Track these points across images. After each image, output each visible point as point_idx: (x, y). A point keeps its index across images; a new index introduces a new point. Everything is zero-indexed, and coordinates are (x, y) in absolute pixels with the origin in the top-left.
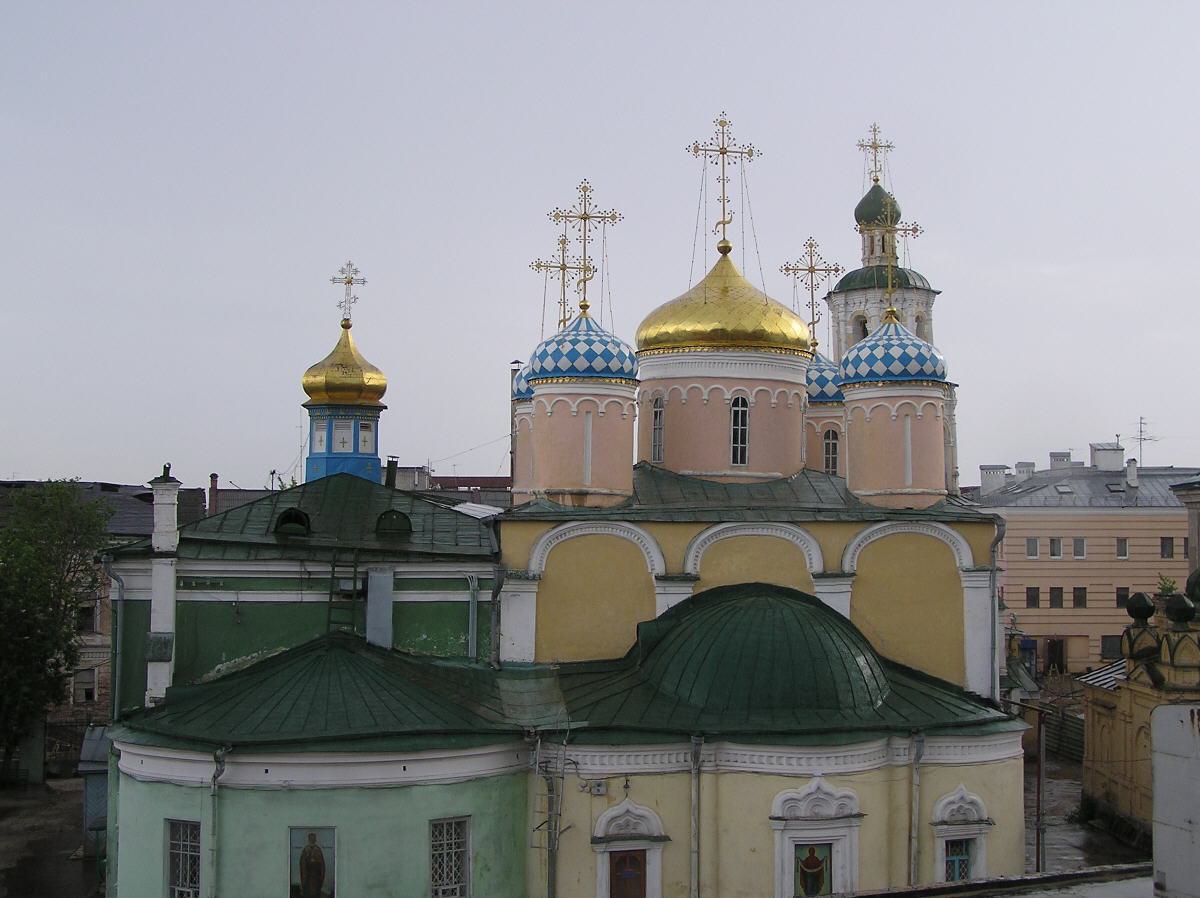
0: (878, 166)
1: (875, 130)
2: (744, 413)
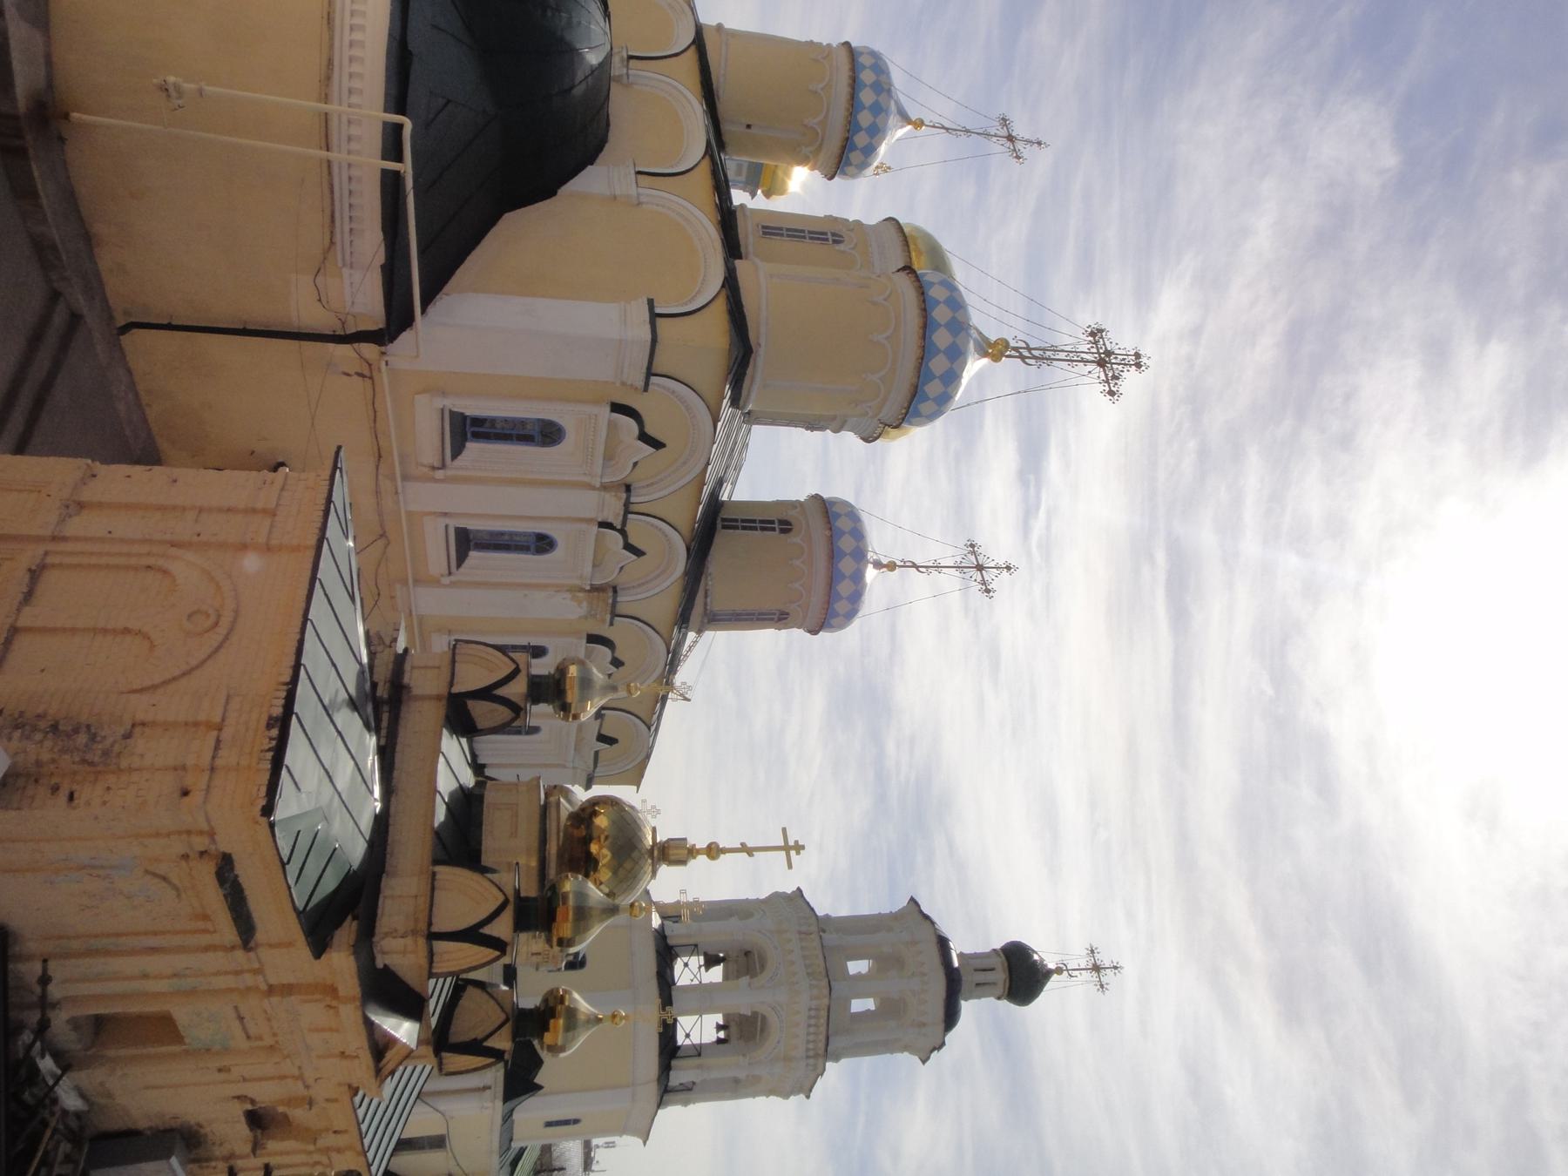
0: (1075, 973)
1: (1115, 968)
2: (827, 240)
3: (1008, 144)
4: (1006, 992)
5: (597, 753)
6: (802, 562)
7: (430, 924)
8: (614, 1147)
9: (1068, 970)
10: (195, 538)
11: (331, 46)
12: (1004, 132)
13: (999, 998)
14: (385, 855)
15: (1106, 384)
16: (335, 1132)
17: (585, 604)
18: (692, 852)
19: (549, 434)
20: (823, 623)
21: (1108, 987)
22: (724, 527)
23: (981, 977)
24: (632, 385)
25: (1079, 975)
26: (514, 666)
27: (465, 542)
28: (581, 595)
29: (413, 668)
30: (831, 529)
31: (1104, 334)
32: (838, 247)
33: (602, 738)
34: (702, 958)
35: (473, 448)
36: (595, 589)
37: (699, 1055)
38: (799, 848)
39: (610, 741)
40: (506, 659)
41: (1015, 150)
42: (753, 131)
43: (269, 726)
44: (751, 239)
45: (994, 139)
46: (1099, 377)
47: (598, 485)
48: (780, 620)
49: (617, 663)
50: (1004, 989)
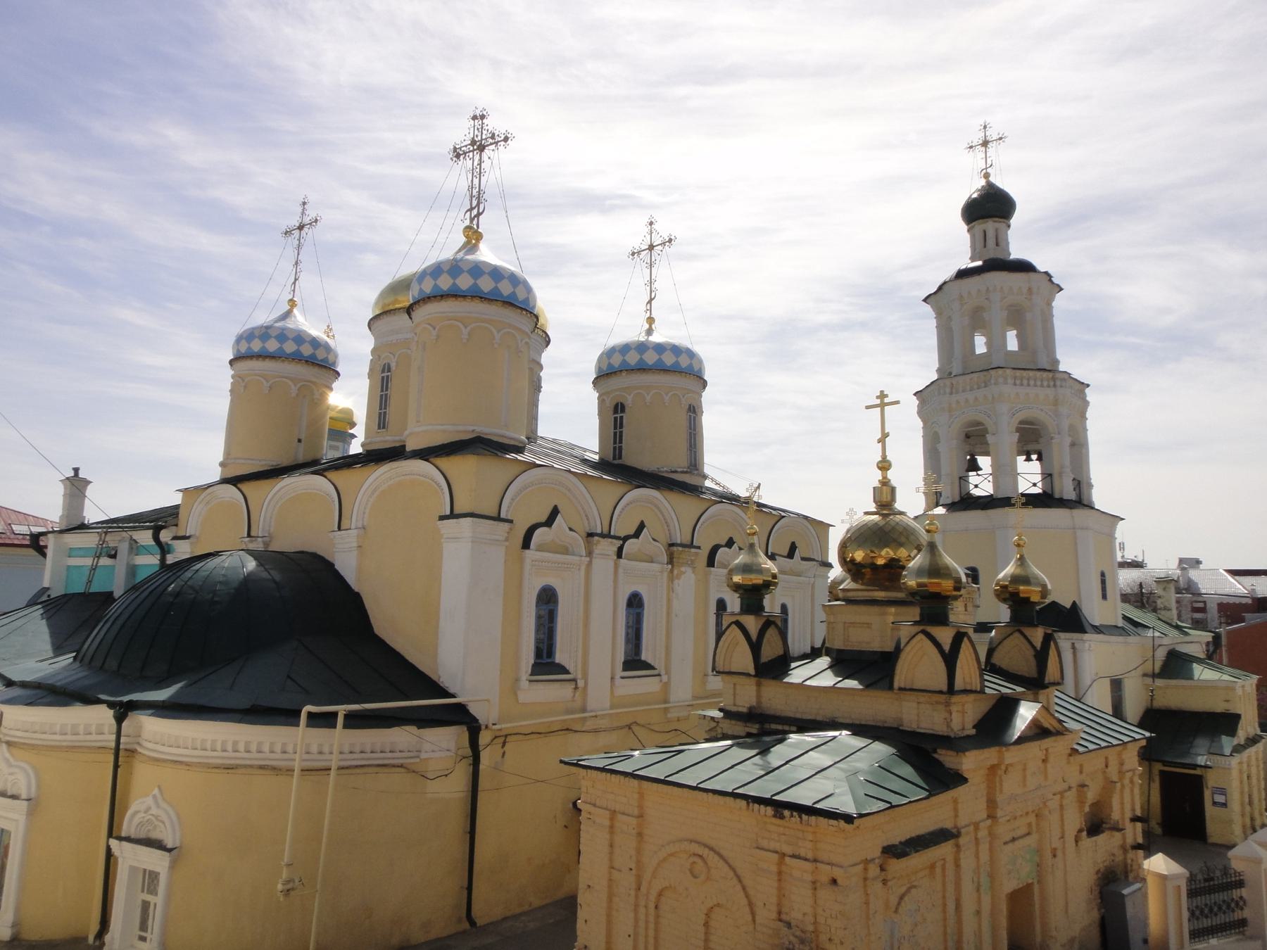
0: (989, 163)
1: (985, 127)
3: (306, 229)
4: (1005, 220)
5: (804, 559)
6: (648, 394)
7: (941, 692)
8: (1123, 544)
9: (986, 168)
10: (634, 872)
11: (251, 766)
12: (296, 233)
13: (1009, 226)
14: (885, 728)
15: (499, 144)
16: (1107, 766)
17: (683, 569)
18: (885, 482)
19: (548, 598)
20: (697, 376)
21: (1001, 133)
22: (620, 457)
23: (991, 242)
24: (508, 533)
25: (991, 159)
26: (734, 626)
27: (634, 663)
28: (675, 572)
29: (735, 705)
30: (621, 371)
31: (457, 147)
32: (393, 368)
33: (791, 555)
34: (971, 473)
35: (559, 657)
36: (671, 561)
37: (1050, 475)
38: (882, 395)
39: (793, 548)
40: (727, 633)
41: (310, 224)
42: (303, 437)
43: (782, 817)
44: (388, 438)
45: (302, 241)
46: (493, 150)
47: (588, 559)
48: (694, 412)
49: (730, 543)
50: (1000, 222)
